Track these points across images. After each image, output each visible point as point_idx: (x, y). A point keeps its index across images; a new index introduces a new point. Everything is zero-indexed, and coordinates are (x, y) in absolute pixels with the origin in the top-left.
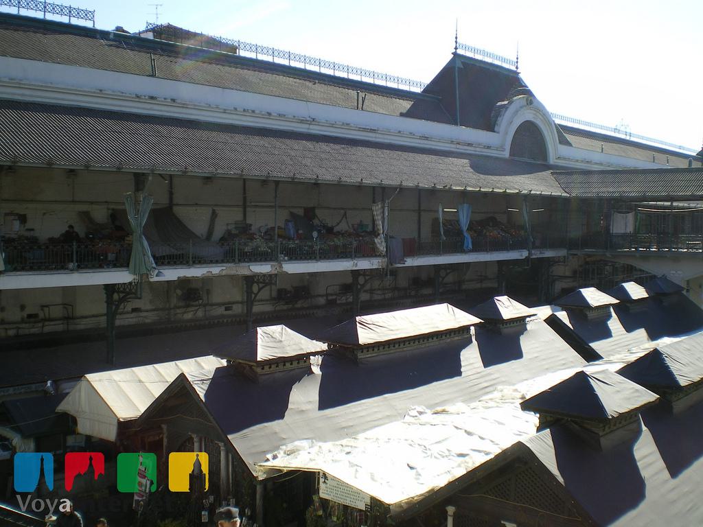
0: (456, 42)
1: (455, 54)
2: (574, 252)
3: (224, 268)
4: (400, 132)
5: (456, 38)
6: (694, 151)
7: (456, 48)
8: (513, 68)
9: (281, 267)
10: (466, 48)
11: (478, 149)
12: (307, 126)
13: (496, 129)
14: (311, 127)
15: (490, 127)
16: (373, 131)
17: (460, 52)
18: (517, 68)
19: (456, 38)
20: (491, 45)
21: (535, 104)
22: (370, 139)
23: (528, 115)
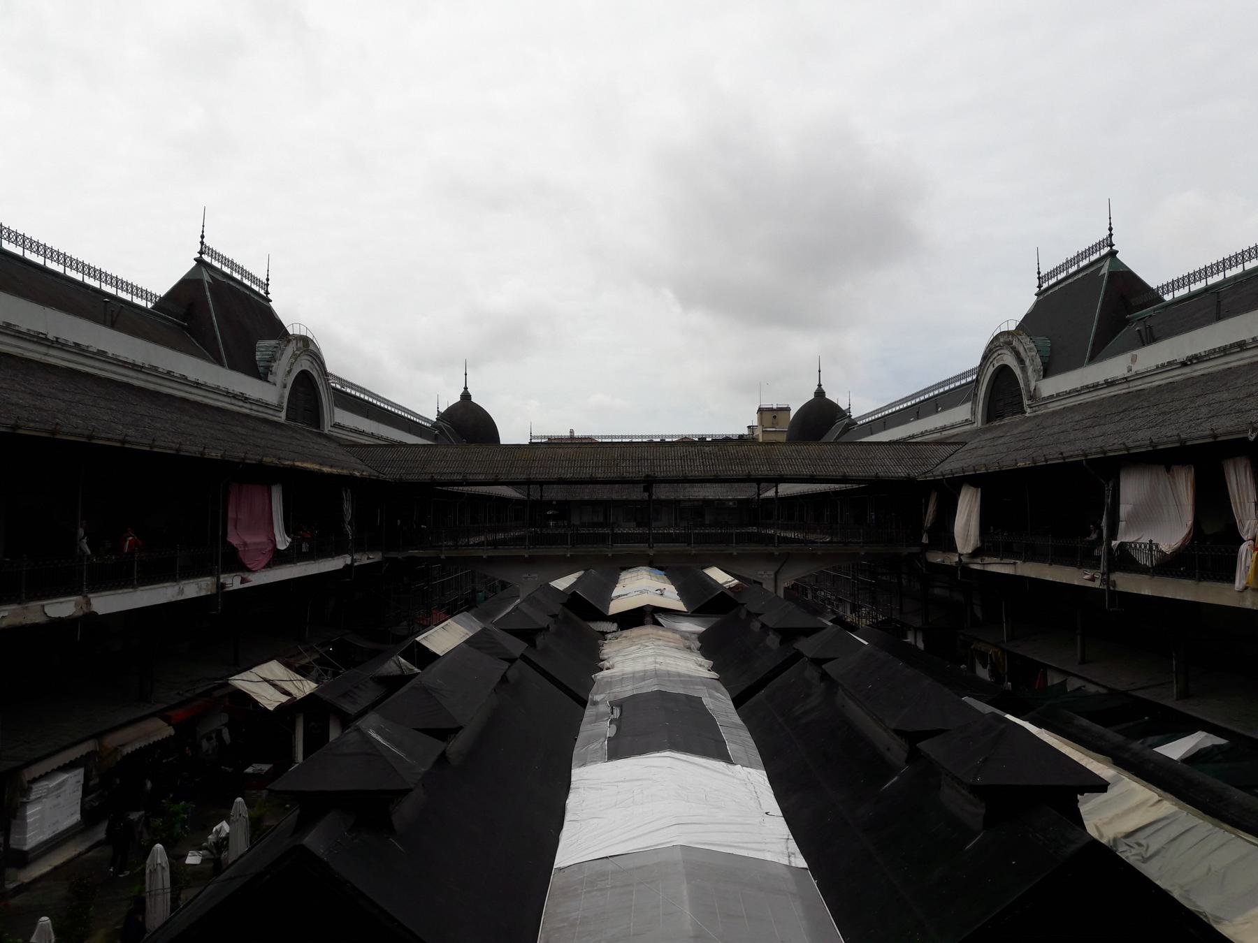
0: (202, 243)
1: (200, 261)
2: (393, 555)
3: (6, 614)
4: (169, 372)
5: (202, 237)
6: (427, 420)
7: (201, 253)
8: (262, 292)
9: (88, 603)
10: (214, 254)
11: (254, 407)
12: (43, 350)
13: (270, 378)
14: (52, 352)
15: (262, 374)
16: (134, 367)
17: (206, 258)
18: (267, 293)
19: (202, 237)
20: (247, 255)
21: (311, 347)
22: (130, 381)
23: (305, 364)
